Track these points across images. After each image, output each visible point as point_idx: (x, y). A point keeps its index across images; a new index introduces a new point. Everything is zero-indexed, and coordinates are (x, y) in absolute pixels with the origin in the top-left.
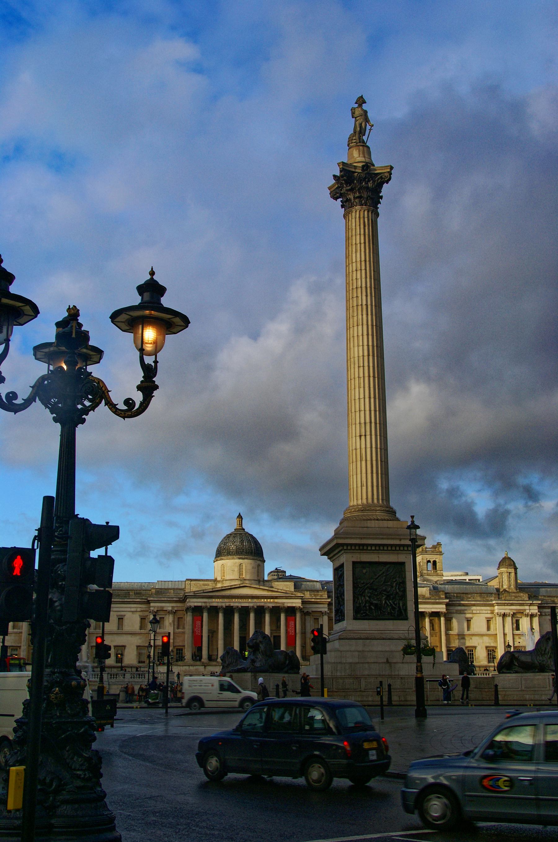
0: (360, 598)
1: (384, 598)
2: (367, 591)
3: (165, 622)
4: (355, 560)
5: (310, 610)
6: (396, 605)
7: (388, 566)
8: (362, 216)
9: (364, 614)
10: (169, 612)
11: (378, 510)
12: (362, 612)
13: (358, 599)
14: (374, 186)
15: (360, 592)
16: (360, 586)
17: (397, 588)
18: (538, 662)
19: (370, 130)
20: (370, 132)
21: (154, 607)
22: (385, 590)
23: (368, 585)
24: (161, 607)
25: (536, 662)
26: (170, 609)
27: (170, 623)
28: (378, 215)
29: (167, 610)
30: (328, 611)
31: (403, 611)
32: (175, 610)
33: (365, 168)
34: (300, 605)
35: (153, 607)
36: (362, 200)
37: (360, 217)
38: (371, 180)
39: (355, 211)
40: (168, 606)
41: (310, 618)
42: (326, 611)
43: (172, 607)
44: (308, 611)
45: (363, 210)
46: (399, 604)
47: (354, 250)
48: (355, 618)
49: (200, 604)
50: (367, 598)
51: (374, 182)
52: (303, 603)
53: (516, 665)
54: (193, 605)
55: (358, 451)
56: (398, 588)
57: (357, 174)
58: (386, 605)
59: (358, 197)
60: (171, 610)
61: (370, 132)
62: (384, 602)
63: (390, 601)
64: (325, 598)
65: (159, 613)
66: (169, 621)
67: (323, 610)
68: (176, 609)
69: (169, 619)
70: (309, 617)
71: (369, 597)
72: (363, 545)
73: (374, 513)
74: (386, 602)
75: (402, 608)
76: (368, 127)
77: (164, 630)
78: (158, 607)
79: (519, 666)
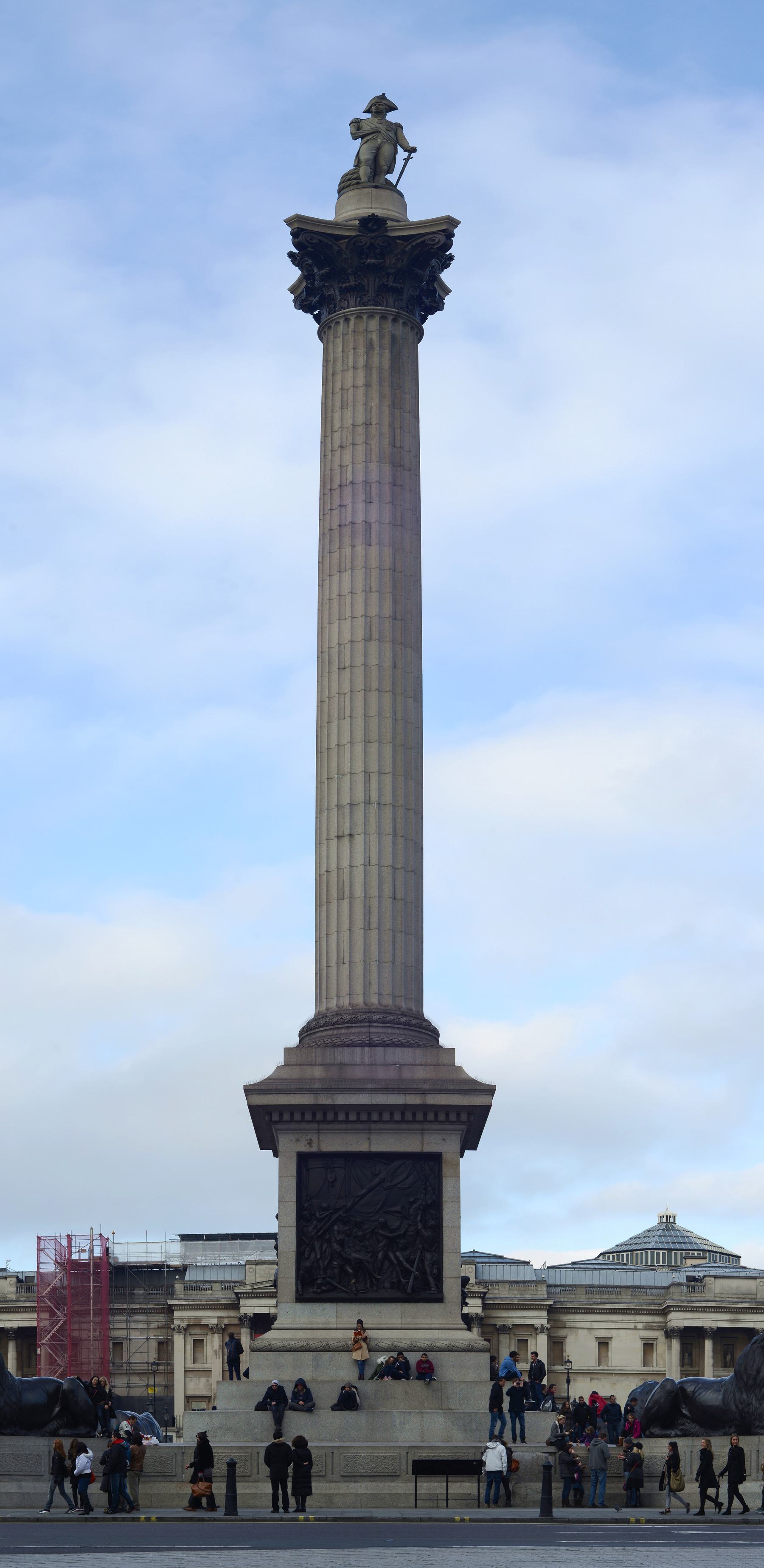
0: (317, 1245)
1: (381, 1244)
2: (336, 1228)
3: (205, 1348)
4: (304, 1148)
5: (509, 1323)
6: (411, 1263)
7: (396, 1163)
9: (324, 1288)
10: (212, 1328)
11: (375, 1022)
12: (319, 1281)
13: (313, 1249)
15: (318, 1232)
16: (318, 1215)
17: (419, 1218)
18: (736, 1406)
21: (182, 1319)
22: (384, 1226)
23: (341, 1213)
24: (196, 1318)
25: (734, 1407)
26: (214, 1321)
27: (215, 1351)
29: (208, 1325)
30: (548, 1323)
31: (431, 1279)
32: (225, 1325)
34: (479, 1310)
35: (179, 1318)
40: (211, 1317)
41: (510, 1339)
42: (542, 1325)
43: (219, 1318)
44: (504, 1325)
46: (422, 1261)
48: (301, 1298)
49: (265, 1311)
50: (335, 1246)
52: (485, 1307)
53: (684, 1416)
54: (250, 1311)
55: (334, 875)
56: (421, 1221)
58: (387, 1264)
60: (217, 1325)
62: (380, 1255)
63: (398, 1254)
64: (542, 1296)
65: (193, 1332)
66: (213, 1347)
67: (537, 1322)
68: (226, 1321)
69: (212, 1341)
70: (508, 1336)
71: (341, 1243)
72: (325, 1109)
73: (365, 1030)
74: (386, 1257)
75: (428, 1270)
77: (203, 1365)
78: (189, 1318)
79: (693, 1420)
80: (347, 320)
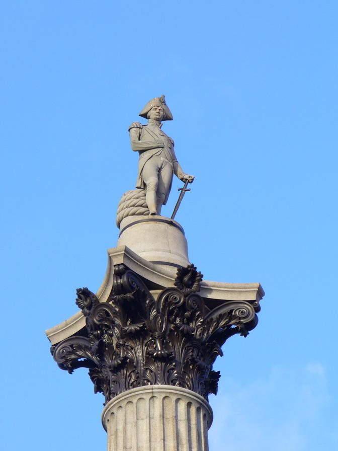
8: (170, 414)
14: (205, 335)
19: (183, 191)
20: (182, 196)
28: (209, 418)
33: (186, 279)
36: (173, 369)
37: (163, 416)
38: (199, 316)
39: (150, 396)
45: (174, 398)
51: (207, 323)
57: (160, 291)
59: (159, 358)
61: (182, 196)
76: (177, 184)
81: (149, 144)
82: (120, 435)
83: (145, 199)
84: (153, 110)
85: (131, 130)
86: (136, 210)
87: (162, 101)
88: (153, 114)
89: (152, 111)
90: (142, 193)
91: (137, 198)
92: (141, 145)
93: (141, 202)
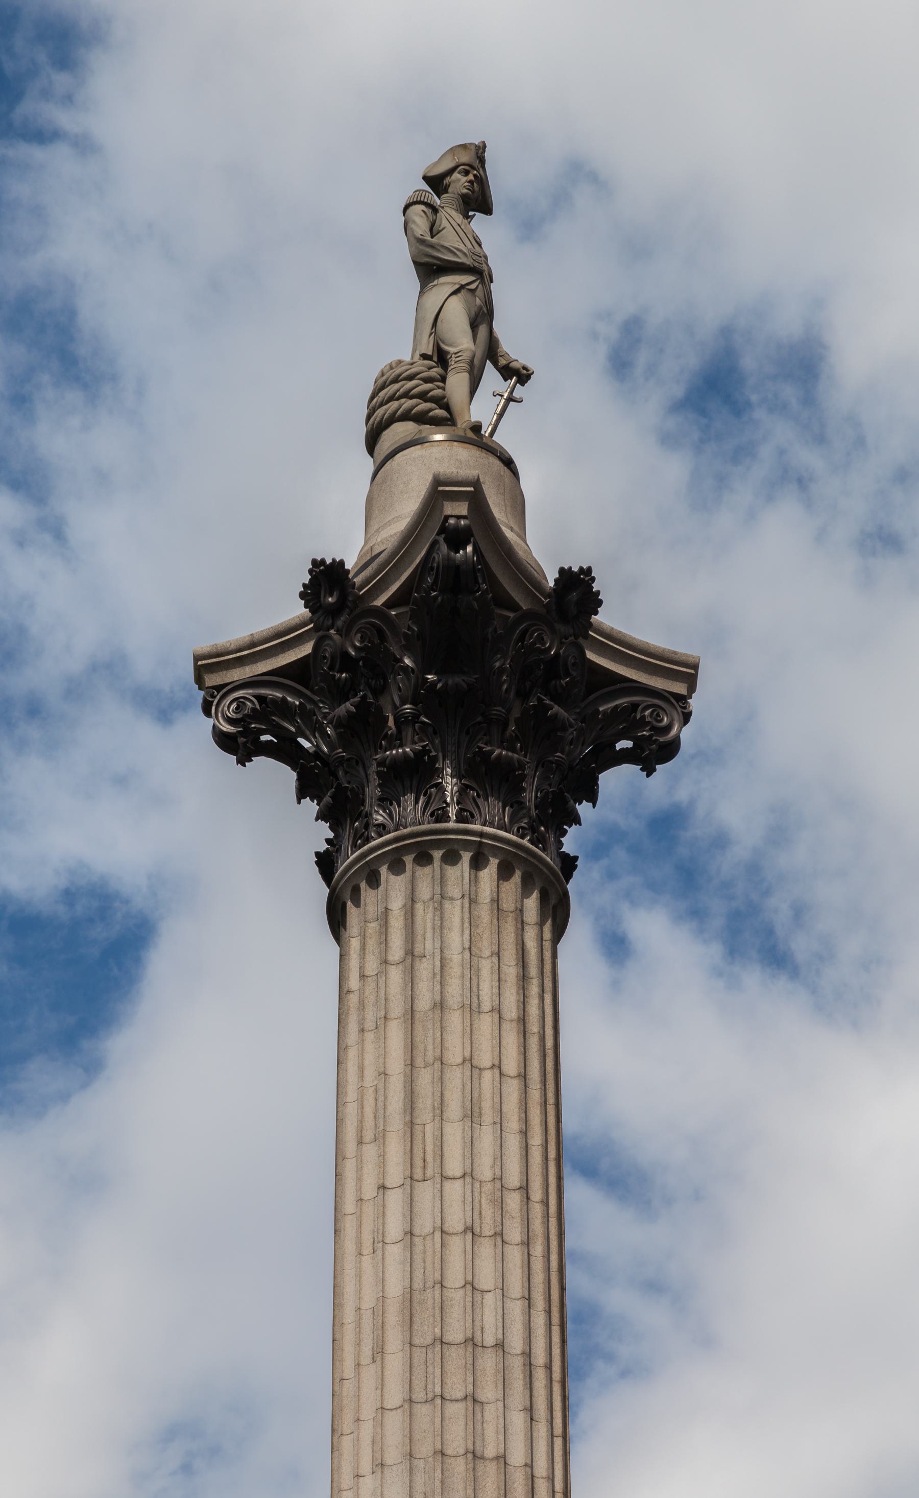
47: (454, 1108)
80: (478, 863)
81: (455, 254)
82: (397, 923)
83: (444, 389)
84: (459, 173)
85: (408, 211)
86: (433, 408)
87: (480, 151)
88: (460, 183)
89: (456, 175)
90: (436, 371)
91: (427, 380)
92: (438, 251)
93: (437, 392)
